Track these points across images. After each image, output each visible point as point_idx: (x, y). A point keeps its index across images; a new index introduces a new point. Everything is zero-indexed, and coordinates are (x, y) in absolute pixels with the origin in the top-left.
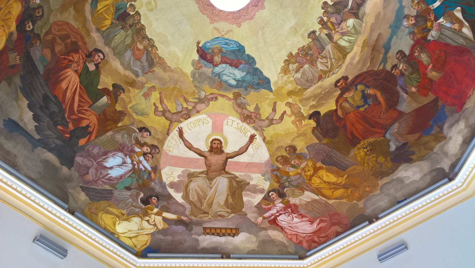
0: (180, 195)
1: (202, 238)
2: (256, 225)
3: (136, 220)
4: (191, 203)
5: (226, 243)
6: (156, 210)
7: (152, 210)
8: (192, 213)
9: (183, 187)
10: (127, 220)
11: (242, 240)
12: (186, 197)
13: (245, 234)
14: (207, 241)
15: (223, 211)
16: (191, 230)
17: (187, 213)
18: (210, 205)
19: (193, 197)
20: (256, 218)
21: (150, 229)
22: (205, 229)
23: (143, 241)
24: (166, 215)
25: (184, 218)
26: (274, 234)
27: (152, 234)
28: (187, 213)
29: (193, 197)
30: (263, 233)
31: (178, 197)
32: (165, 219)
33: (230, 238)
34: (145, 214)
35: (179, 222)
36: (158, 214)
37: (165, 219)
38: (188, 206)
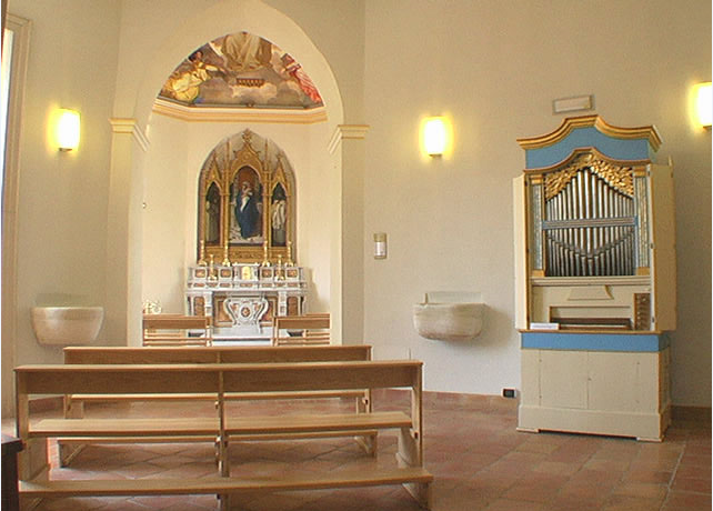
0: (220, 48)
1: (234, 88)
2: (279, 76)
3: (187, 75)
4: (228, 55)
5: (253, 92)
6: (201, 64)
7: (197, 64)
8: (228, 65)
9: (222, 42)
10: (180, 78)
11: (266, 91)
12: (224, 51)
13: (269, 84)
14: (238, 91)
15: (254, 63)
16: (227, 81)
17: (225, 65)
18: (243, 57)
19: (230, 51)
20: (280, 70)
21: (198, 81)
22: (238, 80)
23: (192, 94)
24: (208, 67)
25: (222, 70)
26: (292, 84)
27: (199, 86)
28: (225, 65)
29: (230, 51)
30: (283, 83)
31: (218, 51)
32: (207, 71)
33: (256, 88)
34: (194, 69)
35: (219, 73)
36: (203, 67)
37: (207, 71)
38: (225, 59)
